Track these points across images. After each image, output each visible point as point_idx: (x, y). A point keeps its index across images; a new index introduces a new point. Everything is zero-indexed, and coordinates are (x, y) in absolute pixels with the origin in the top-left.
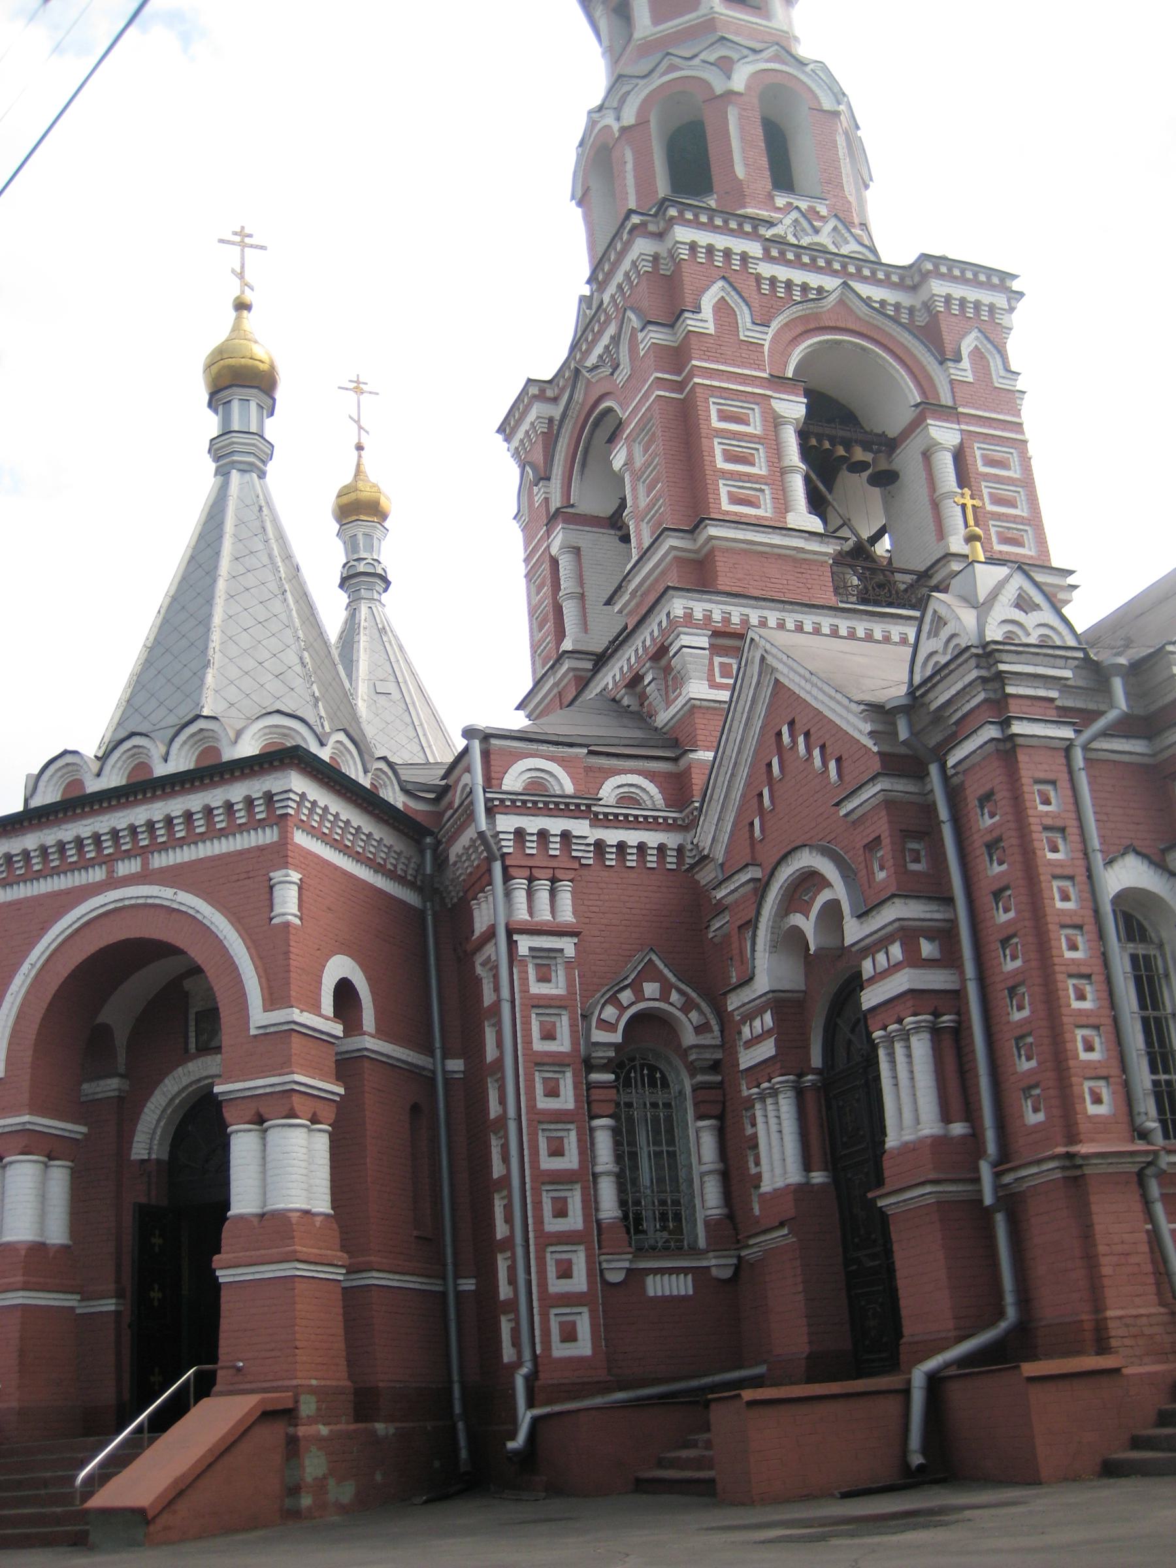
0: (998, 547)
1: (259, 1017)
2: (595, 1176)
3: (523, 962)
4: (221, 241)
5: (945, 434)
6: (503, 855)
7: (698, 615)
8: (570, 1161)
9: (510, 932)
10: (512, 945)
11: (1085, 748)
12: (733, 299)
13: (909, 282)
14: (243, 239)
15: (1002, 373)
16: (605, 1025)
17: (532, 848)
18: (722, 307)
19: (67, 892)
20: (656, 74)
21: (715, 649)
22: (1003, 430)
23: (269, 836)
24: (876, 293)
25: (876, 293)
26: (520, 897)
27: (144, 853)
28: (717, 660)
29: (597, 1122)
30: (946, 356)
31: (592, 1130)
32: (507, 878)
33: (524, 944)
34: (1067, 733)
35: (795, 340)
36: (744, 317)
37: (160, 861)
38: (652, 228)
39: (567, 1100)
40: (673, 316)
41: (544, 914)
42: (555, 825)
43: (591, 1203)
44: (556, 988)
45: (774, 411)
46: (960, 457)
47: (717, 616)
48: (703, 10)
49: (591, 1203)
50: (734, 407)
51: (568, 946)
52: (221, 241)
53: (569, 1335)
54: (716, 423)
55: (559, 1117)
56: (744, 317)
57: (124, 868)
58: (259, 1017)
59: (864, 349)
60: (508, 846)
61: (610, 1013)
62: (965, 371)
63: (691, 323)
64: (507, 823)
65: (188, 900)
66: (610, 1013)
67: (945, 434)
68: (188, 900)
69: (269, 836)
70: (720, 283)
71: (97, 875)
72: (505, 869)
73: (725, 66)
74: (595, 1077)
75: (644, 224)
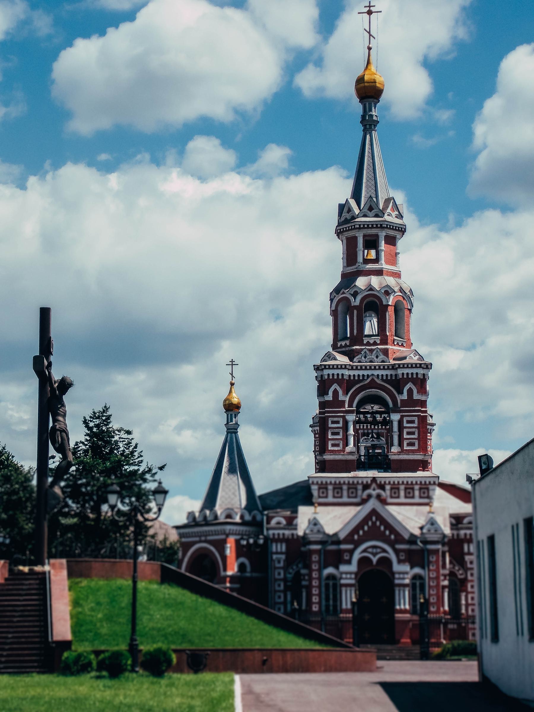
7: (315, 482)
8: (282, 599)
12: (338, 389)
16: (290, 573)
18: (335, 392)
20: (340, 294)
24: (384, 372)
25: (384, 372)
27: (206, 536)
30: (400, 392)
33: (274, 557)
36: (340, 392)
39: (282, 587)
43: (285, 608)
46: (400, 422)
47: (320, 482)
48: (357, 264)
49: (285, 608)
50: (336, 419)
55: (280, 591)
56: (340, 392)
61: (291, 571)
64: (271, 532)
65: (212, 548)
66: (291, 571)
68: (212, 548)
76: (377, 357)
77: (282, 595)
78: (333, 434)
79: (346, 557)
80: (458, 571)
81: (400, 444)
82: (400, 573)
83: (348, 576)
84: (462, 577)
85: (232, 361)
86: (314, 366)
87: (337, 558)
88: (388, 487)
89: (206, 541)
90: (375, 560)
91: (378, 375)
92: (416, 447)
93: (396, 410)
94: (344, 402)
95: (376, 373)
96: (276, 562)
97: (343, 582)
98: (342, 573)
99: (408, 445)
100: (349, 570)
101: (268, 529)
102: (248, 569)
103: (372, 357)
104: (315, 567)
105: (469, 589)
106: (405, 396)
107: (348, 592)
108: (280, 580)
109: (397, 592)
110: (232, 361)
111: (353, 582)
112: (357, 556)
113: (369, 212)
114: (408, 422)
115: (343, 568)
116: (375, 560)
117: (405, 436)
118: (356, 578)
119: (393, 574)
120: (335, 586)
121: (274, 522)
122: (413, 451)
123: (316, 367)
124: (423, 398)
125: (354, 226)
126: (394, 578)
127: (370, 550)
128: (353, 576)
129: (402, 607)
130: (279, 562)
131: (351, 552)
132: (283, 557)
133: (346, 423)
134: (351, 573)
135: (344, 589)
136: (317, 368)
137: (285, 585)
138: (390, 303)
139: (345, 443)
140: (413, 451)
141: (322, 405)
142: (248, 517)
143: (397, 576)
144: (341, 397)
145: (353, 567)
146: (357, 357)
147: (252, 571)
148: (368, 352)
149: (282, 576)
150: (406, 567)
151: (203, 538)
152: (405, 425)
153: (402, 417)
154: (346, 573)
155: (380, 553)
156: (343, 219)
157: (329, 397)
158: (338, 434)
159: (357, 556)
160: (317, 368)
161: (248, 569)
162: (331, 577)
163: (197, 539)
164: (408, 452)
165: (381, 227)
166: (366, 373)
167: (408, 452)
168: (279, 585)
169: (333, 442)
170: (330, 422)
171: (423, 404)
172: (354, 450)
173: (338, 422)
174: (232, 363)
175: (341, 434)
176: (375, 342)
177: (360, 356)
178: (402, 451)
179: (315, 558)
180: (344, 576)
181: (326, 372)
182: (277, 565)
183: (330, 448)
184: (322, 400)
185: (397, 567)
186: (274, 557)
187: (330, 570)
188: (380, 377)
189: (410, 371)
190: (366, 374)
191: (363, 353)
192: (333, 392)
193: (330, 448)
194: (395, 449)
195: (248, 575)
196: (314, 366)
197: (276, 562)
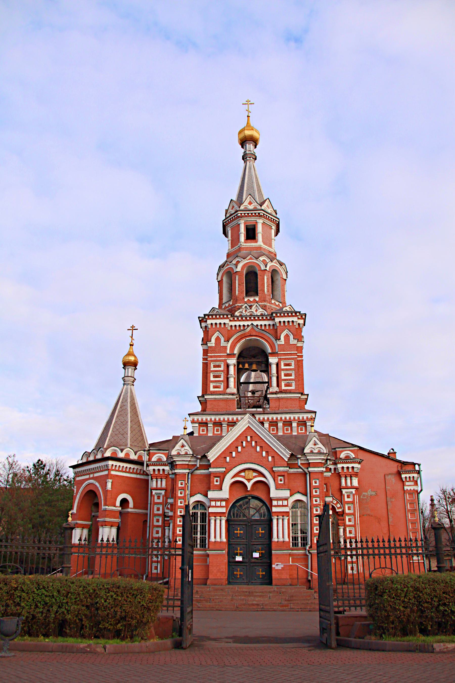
0: (283, 388)
1: (103, 507)
2: (165, 538)
3: (154, 496)
4: (128, 330)
6: (151, 475)
8: (160, 535)
9: (151, 490)
10: (151, 492)
11: (192, 473)
12: (221, 336)
13: (272, 318)
14: (133, 328)
15: (293, 340)
17: (156, 473)
18: (218, 339)
19: (83, 480)
20: (225, 267)
21: (200, 426)
22: (291, 356)
23: (106, 473)
24: (263, 323)
26: (154, 482)
28: (201, 428)
29: (166, 528)
30: (278, 338)
31: (165, 529)
32: (152, 479)
33: (154, 492)
34: (188, 471)
35: (238, 341)
36: (222, 339)
37: (96, 475)
38: (204, 320)
39: (160, 523)
41: (159, 486)
42: (161, 468)
44: (161, 500)
45: (227, 363)
46: (278, 365)
47: (200, 419)
48: (239, 244)
50: (217, 363)
51: (163, 492)
52: (128, 330)
53: (156, 568)
54: (212, 369)
55: (158, 526)
56: (222, 339)
57: (91, 476)
58: (103, 507)
59: (257, 339)
60: (152, 473)
62: (282, 341)
63: (209, 344)
64: (151, 468)
69: (106, 473)
70: (217, 332)
71: (87, 477)
72: (151, 477)
74: (166, 519)
75: (203, 319)
76: (256, 311)
77: (160, 530)
78: (215, 377)
80: (336, 504)
81: (278, 386)
82: (278, 499)
83: (218, 504)
84: (340, 510)
85: (133, 327)
86: (199, 317)
87: (207, 484)
88: (266, 425)
89: (93, 478)
90: (249, 485)
91: (257, 325)
92: (293, 388)
93: (274, 354)
94: (226, 347)
95: (255, 323)
96: (156, 497)
97: (211, 510)
98: (211, 500)
99: (286, 385)
101: (148, 465)
102: (131, 504)
103: (252, 311)
105: (348, 523)
106: (282, 341)
107: (218, 522)
108: (159, 515)
109: (275, 522)
110: (133, 327)
111: (224, 510)
112: (228, 481)
113: (249, 205)
114: (286, 365)
115: (211, 494)
116: (249, 485)
117: (283, 377)
118: (226, 507)
119: (271, 500)
120: (203, 515)
121: (154, 459)
122: (290, 392)
123: (200, 319)
124: (299, 344)
125: (237, 215)
126: (271, 506)
127: (243, 474)
128: (224, 503)
129: (281, 539)
130: (159, 498)
131: (222, 476)
132: (163, 492)
133: (228, 366)
134: (221, 500)
135: (213, 519)
136: (202, 320)
137: (164, 521)
138: (268, 269)
139: (226, 384)
140: (290, 392)
141: (205, 352)
142: (133, 457)
143: (274, 503)
144: (223, 343)
145: (225, 493)
146: (238, 311)
147: (135, 507)
148: (248, 307)
149: (161, 512)
150: (286, 493)
151: (91, 476)
152: (283, 367)
153: (280, 360)
154: (216, 500)
155: (255, 477)
156: (228, 215)
157: (212, 343)
158: (219, 376)
159: (228, 481)
160: (202, 320)
161: (131, 504)
163: (87, 477)
164: (286, 392)
165: (259, 216)
166: (246, 323)
167: (286, 392)
168: (158, 521)
169: (215, 384)
170: (212, 366)
171: (300, 349)
172: (235, 391)
173: (219, 366)
174: (133, 328)
175: (222, 376)
176: (255, 300)
177: (241, 310)
178: (281, 392)
180: (213, 503)
181: (209, 322)
182: (156, 500)
183: (212, 389)
184: (205, 347)
185: (274, 493)
186: (154, 492)
187: (199, 497)
188: (259, 327)
189: (286, 319)
190: (246, 325)
191: (243, 307)
192: (216, 339)
193: (212, 389)
194: (274, 388)
195: (129, 510)
196: (199, 317)
197: (156, 497)
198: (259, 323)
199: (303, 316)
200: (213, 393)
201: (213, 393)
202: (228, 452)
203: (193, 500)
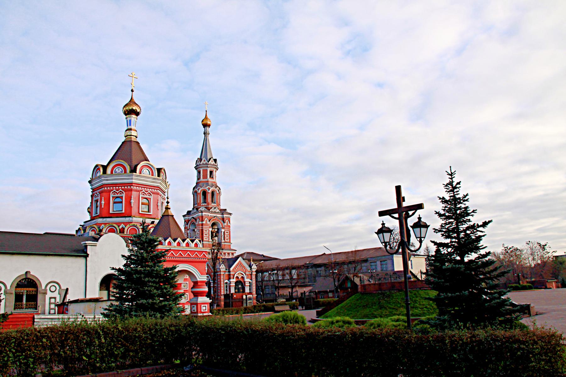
5: (223, 230)
30: (224, 222)
40: (202, 221)
62: (225, 224)
67: (223, 230)
73: (209, 189)
79: (232, 277)
90: (240, 277)
93: (223, 228)
100: (233, 280)
104: (222, 280)
112: (235, 276)
116: (240, 277)
119: (245, 282)
131: (234, 275)
162: (226, 283)
171: (229, 226)
178: (225, 242)
179: (222, 277)
185: (246, 280)
194: (223, 241)
198: (218, 215)
199: (230, 214)
200: (205, 241)
201: (205, 241)
202: (235, 268)
203: (225, 281)
